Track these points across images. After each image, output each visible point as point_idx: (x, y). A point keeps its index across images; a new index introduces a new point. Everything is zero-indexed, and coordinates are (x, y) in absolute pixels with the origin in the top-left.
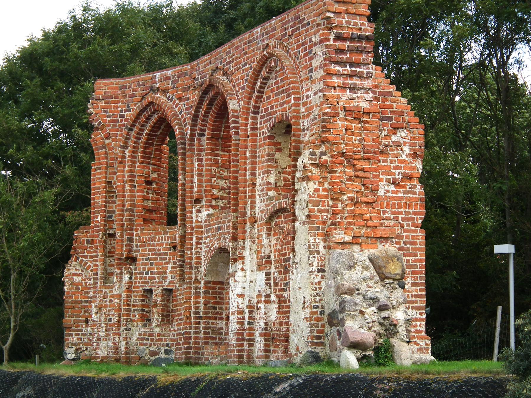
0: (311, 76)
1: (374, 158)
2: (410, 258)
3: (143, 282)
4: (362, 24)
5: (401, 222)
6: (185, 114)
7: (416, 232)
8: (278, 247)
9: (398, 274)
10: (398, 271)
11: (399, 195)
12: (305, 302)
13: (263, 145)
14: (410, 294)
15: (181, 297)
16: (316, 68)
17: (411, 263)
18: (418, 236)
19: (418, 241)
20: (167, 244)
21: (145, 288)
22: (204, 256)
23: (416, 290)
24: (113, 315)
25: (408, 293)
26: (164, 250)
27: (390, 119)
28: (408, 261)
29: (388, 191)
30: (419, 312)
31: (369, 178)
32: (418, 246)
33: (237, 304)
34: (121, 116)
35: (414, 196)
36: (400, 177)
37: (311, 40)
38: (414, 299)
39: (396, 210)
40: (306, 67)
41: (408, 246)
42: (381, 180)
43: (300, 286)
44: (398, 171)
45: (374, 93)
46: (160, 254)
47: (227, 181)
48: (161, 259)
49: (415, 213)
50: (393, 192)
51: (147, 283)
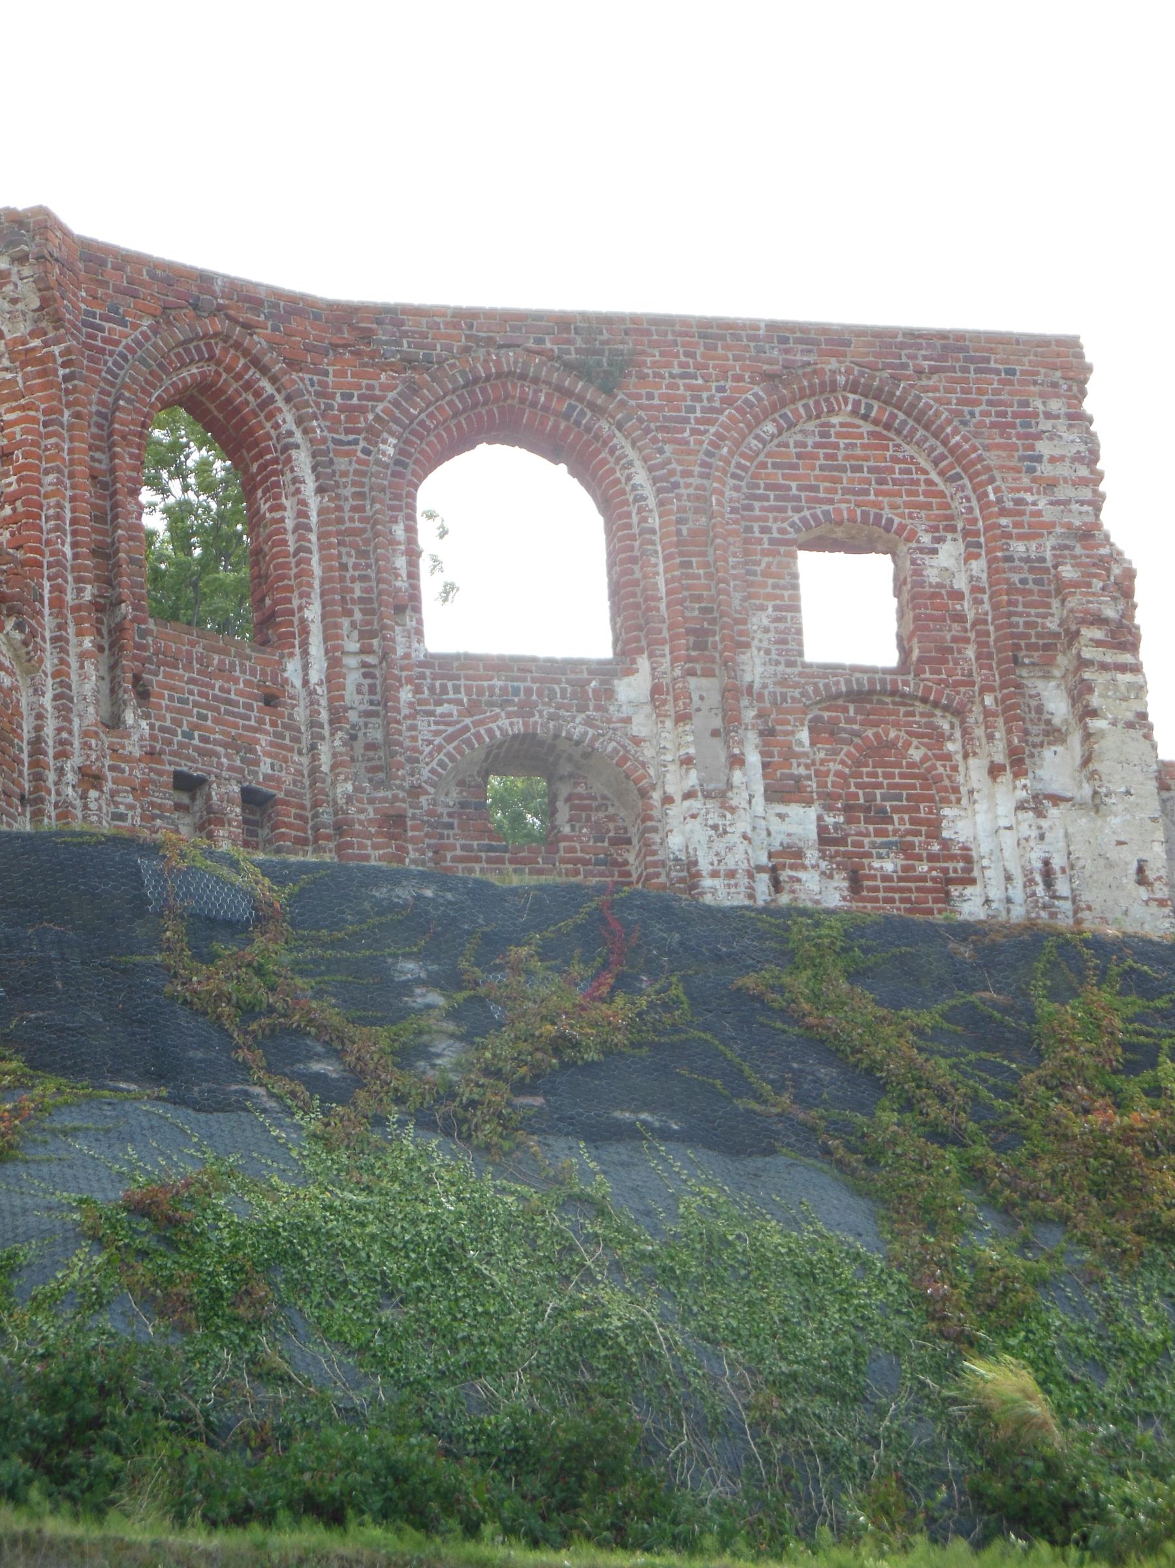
0: (1034, 470)
3: (173, 754)
6: (318, 405)
8: (834, 767)
12: (1140, 870)
13: (765, 553)
15: (362, 817)
16: (1053, 460)
20: (247, 683)
21: (185, 769)
22: (429, 742)
24: (131, 807)
26: (240, 693)
33: (740, 856)
34: (85, 324)
37: (1026, 404)
40: (1014, 448)
43: (1122, 839)
46: (229, 702)
48: (228, 712)
51: (194, 761)
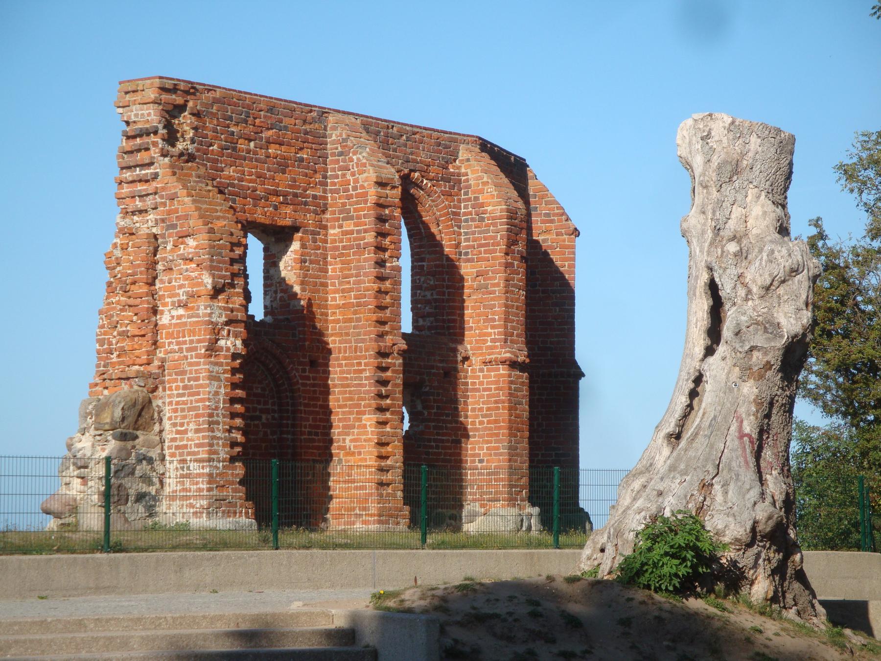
1: (140, 280)
2: (193, 398)
4: (149, 115)
5: (185, 354)
7: (198, 364)
9: (107, 423)
10: (108, 420)
11: (184, 320)
14: (193, 443)
17: (194, 405)
18: (201, 369)
19: (201, 375)
23: (198, 438)
25: (190, 443)
27: (174, 226)
28: (191, 401)
29: (173, 317)
30: (201, 465)
31: (137, 306)
32: (201, 382)
35: (197, 319)
36: (185, 298)
38: (196, 450)
39: (181, 339)
41: (192, 383)
42: (165, 305)
44: (183, 290)
45: (162, 197)
47: (434, 292)
49: (199, 341)
50: (179, 317)
